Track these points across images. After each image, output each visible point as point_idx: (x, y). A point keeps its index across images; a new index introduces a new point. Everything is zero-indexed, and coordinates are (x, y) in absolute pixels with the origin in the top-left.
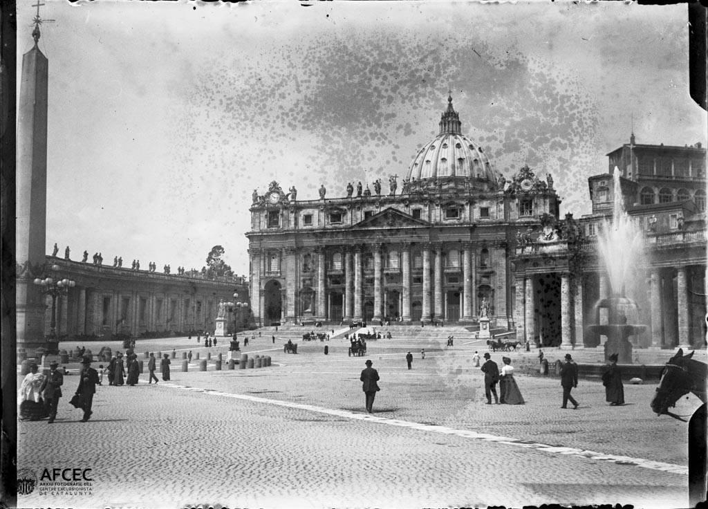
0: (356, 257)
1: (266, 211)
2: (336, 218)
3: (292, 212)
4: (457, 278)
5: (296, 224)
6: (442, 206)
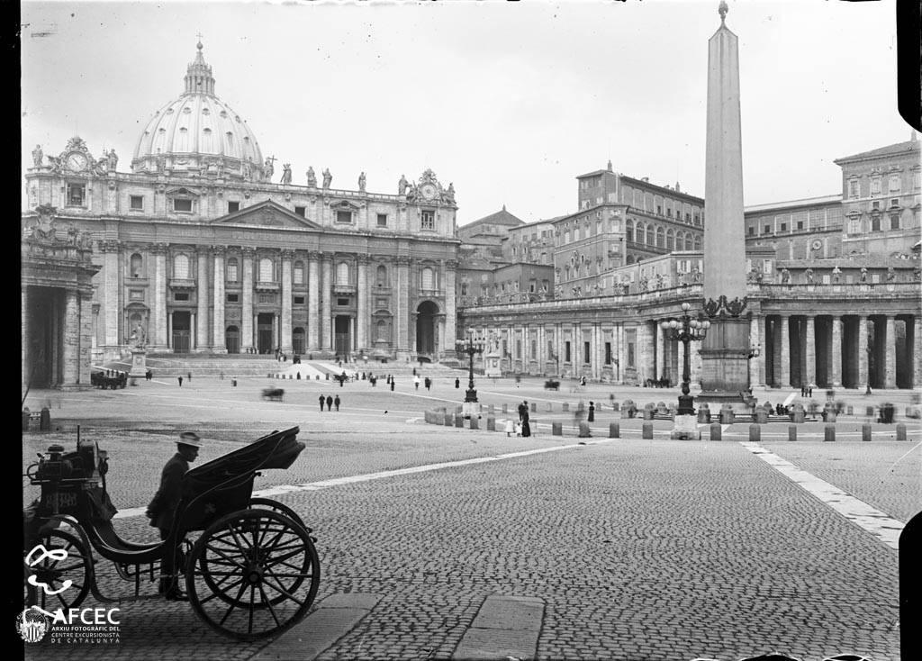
1: (63, 181)
2: (183, 205)
3: (112, 189)
4: (348, 300)
5: (118, 208)
6: (332, 206)
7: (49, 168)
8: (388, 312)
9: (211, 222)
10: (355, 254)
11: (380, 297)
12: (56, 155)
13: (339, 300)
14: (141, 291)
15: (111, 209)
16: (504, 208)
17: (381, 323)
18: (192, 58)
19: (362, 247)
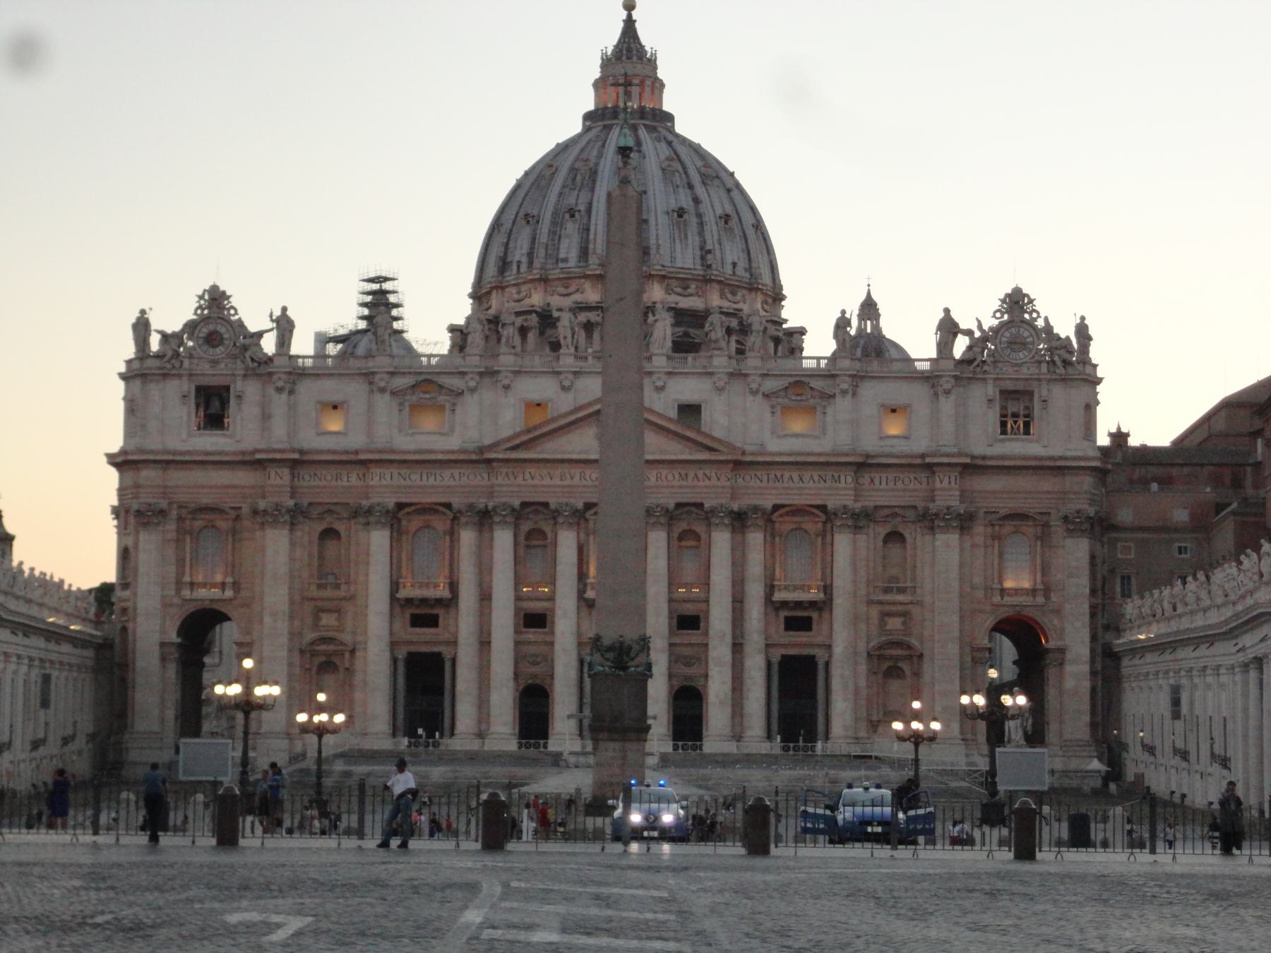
0: (503, 540)
3: (279, 390)
4: (809, 619)
7: (158, 356)
8: (910, 647)
9: (481, 450)
10: (823, 508)
11: (894, 608)
12: (174, 326)
13: (786, 618)
14: (338, 611)
15: (279, 435)
17: (894, 672)
18: (610, 38)
19: (839, 493)
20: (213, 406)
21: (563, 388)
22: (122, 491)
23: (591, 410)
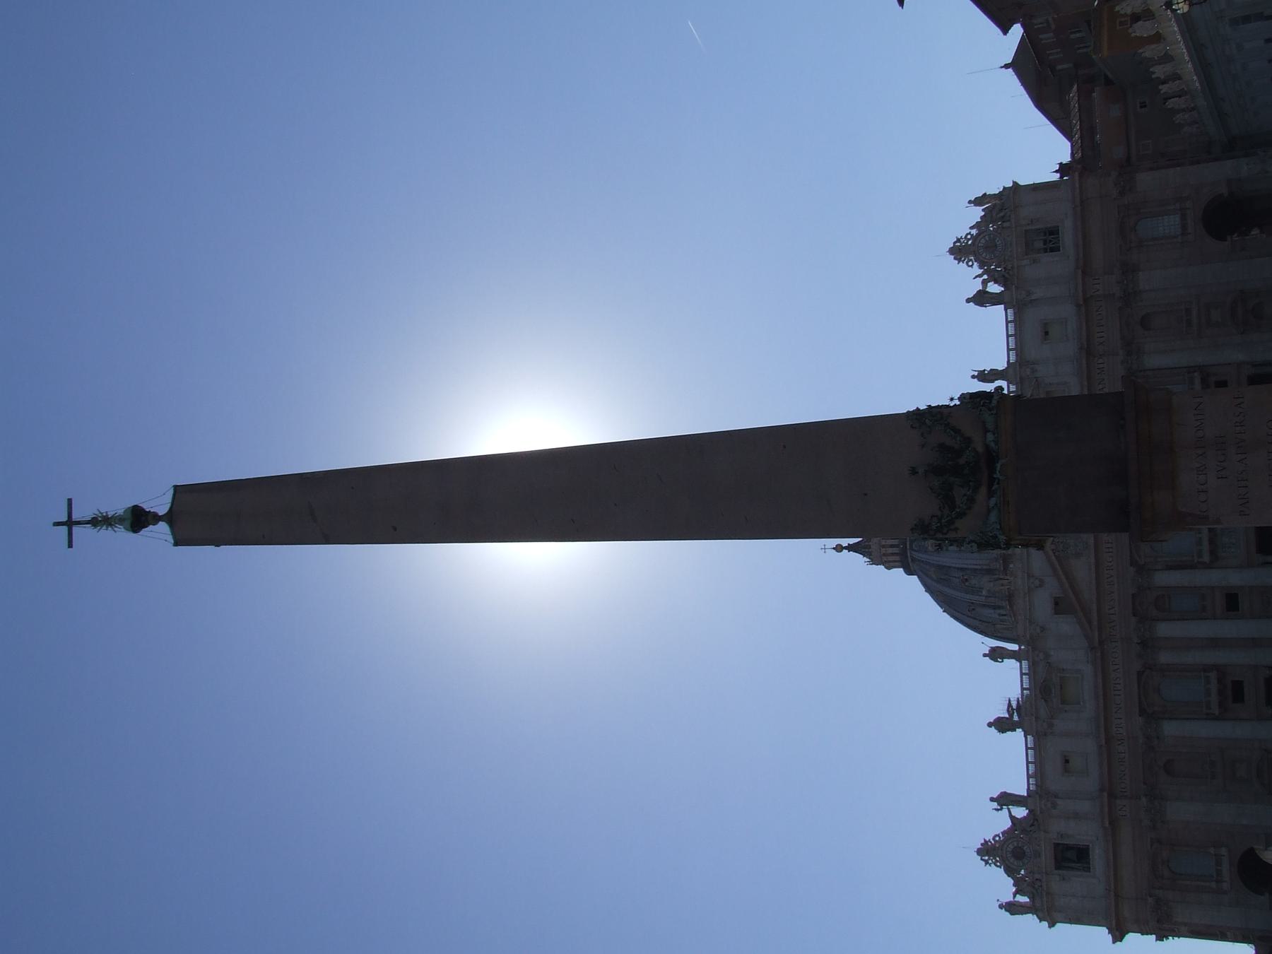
0: (1165, 629)
3: (1054, 806)
7: (1032, 898)
16: (1006, 66)
20: (1072, 857)
21: (1041, 586)
22: (1144, 932)
23: (1056, 563)
